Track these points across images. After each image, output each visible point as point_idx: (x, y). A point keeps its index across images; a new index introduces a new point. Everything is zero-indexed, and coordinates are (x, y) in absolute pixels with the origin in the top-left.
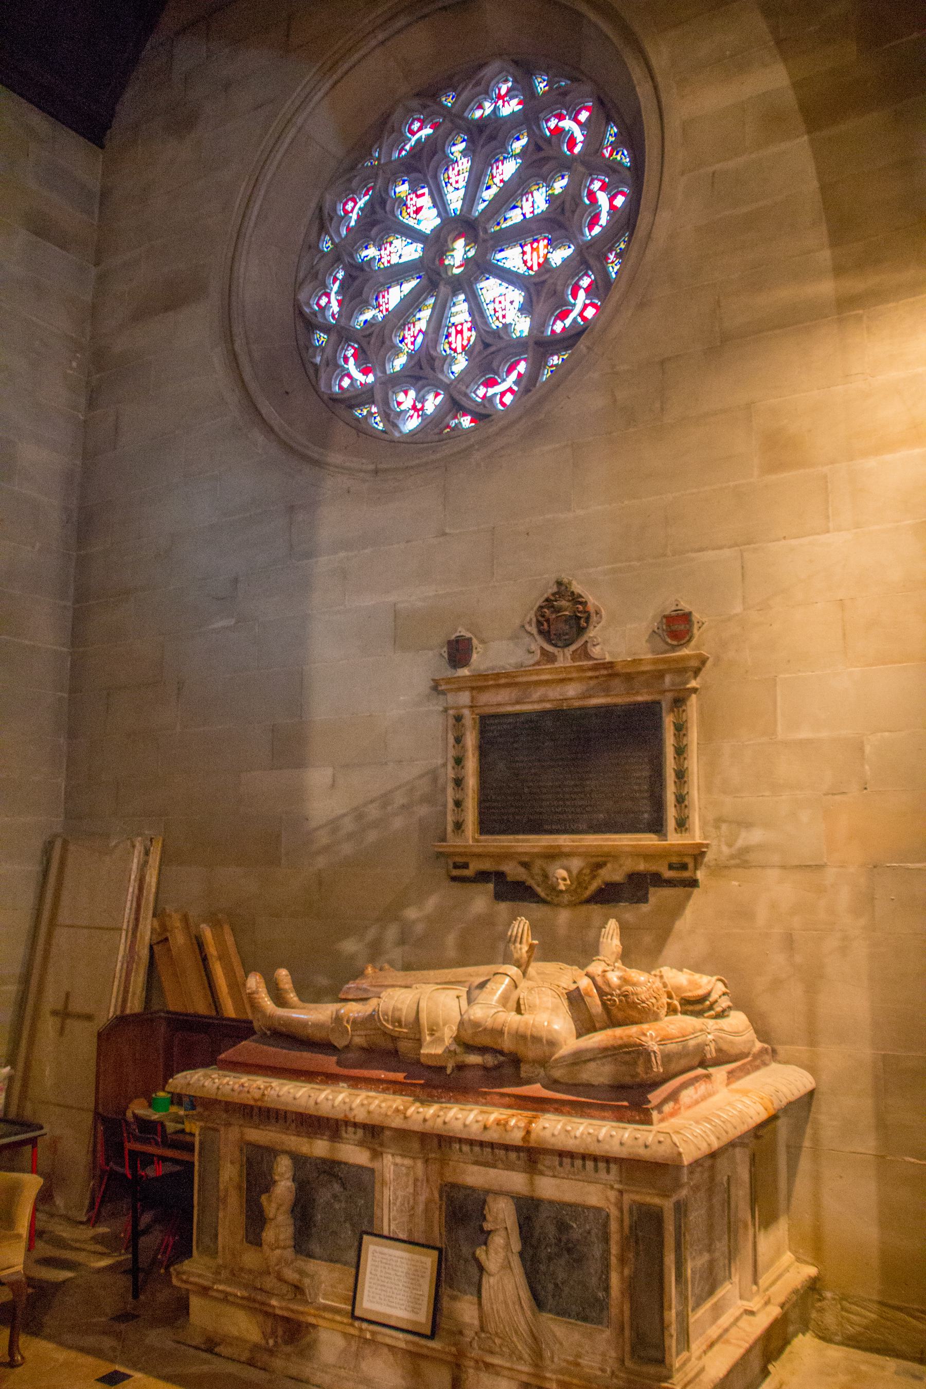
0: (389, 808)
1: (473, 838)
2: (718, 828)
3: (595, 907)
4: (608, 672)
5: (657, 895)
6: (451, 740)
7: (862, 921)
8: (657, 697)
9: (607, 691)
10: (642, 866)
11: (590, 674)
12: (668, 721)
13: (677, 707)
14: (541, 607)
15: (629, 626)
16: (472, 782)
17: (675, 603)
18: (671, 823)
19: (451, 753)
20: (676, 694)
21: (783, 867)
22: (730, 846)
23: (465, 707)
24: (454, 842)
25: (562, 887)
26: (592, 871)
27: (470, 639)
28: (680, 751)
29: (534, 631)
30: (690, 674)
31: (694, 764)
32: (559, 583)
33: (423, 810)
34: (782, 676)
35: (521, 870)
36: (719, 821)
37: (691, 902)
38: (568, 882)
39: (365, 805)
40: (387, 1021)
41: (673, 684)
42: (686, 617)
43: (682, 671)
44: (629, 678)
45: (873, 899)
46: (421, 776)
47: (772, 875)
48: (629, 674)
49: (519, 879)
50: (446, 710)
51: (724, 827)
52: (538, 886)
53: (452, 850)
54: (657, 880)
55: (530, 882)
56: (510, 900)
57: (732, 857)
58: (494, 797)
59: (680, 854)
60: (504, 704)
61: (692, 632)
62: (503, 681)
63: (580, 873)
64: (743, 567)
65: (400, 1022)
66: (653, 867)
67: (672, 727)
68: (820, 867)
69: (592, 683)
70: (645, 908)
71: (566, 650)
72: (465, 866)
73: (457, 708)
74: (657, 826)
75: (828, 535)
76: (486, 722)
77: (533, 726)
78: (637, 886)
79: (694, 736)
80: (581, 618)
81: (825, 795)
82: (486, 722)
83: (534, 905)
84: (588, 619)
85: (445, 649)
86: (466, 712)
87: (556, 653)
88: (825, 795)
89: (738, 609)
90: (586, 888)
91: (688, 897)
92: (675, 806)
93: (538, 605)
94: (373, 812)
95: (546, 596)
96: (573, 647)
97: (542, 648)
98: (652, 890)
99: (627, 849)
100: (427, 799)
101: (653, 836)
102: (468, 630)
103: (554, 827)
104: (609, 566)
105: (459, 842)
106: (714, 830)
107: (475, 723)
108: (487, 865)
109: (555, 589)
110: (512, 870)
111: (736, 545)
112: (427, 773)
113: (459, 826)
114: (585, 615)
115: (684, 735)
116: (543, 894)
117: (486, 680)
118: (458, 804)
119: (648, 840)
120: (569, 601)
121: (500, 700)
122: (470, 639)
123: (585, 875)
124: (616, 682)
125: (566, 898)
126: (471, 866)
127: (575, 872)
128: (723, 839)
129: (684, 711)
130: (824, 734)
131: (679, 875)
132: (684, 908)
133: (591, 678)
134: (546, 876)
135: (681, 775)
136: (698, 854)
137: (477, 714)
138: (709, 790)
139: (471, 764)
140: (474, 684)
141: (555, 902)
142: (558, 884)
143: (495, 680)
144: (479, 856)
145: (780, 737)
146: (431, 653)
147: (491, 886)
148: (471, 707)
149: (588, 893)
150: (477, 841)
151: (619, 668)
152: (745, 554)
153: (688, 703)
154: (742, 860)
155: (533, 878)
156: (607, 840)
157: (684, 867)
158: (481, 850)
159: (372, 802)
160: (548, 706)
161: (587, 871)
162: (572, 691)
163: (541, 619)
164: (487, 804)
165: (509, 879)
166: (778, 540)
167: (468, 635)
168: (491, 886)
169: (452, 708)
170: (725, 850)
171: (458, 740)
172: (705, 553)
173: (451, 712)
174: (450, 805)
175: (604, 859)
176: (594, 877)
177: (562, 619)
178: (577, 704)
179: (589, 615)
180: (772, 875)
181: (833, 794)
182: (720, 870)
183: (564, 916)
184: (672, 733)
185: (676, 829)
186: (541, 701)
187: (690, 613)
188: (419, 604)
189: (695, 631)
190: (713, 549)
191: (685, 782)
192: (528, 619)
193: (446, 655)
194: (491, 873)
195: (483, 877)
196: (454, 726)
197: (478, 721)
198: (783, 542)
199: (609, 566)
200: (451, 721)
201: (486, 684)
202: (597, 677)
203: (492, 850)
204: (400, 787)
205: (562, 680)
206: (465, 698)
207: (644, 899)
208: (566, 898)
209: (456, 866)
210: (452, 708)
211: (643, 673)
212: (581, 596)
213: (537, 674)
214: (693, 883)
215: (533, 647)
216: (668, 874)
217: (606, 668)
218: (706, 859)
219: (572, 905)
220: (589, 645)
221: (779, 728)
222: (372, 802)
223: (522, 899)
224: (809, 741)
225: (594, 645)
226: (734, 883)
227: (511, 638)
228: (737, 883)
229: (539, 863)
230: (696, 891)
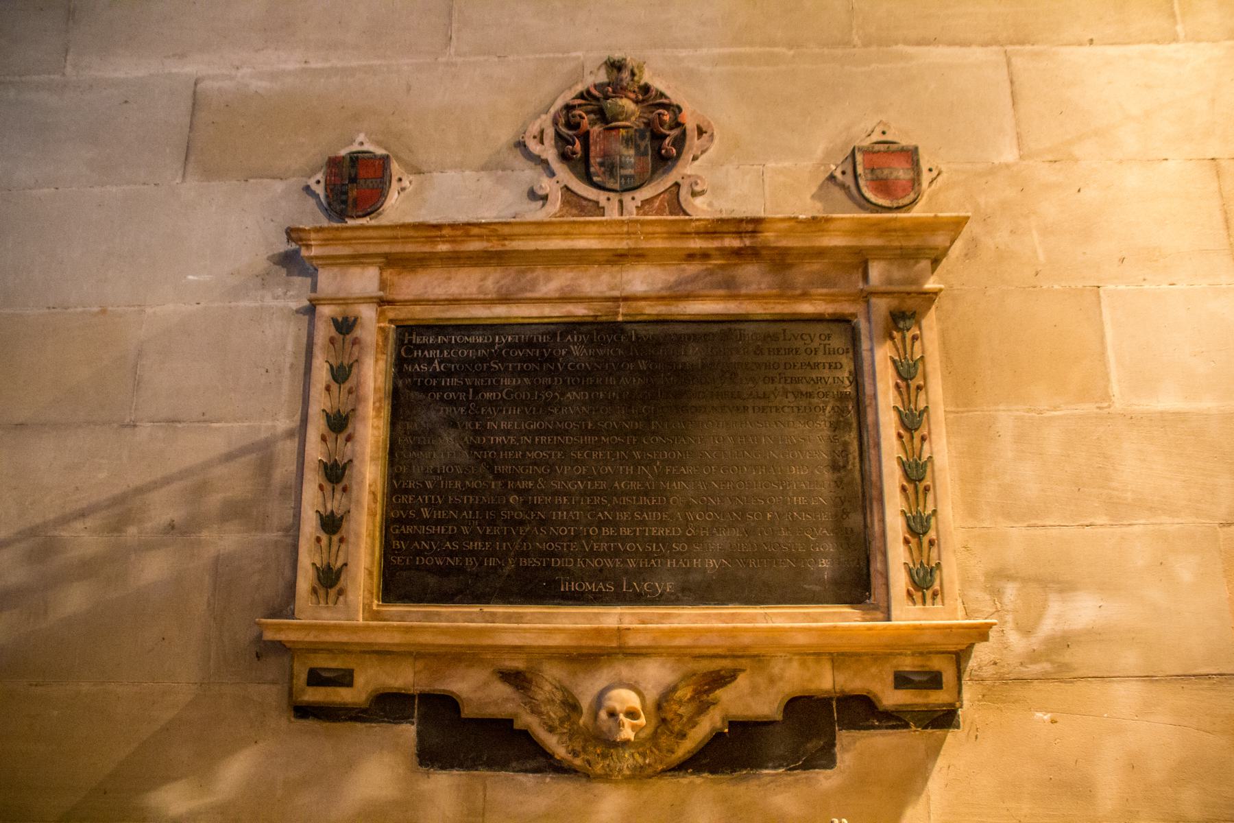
0: (132, 530)
1: (367, 607)
2: (996, 593)
3: (697, 780)
4: (744, 241)
5: (856, 749)
6: (321, 374)
8: (847, 308)
9: (731, 289)
10: (826, 681)
11: (697, 244)
12: (882, 357)
13: (898, 329)
14: (568, 108)
15: (771, 165)
16: (370, 473)
17: (878, 130)
18: (899, 581)
19: (320, 403)
20: (894, 303)
21: (1149, 678)
22: (1027, 632)
23: (367, 300)
24: (312, 617)
25: (627, 733)
26: (698, 693)
27: (385, 160)
28: (912, 422)
29: (549, 152)
30: (925, 264)
31: (942, 450)
32: (615, 66)
33: (227, 540)
34: (1111, 287)
35: (501, 690)
36: (997, 577)
37: (941, 762)
38: (642, 721)
39: (64, 520)
41: (890, 281)
42: (911, 155)
43: (907, 256)
44: (781, 260)
46: (229, 457)
48: (784, 252)
49: (491, 712)
50: (311, 310)
51: (1011, 591)
52: (551, 730)
53: (311, 637)
54: (862, 711)
55: (527, 720)
56: (461, 766)
57: (1033, 657)
58: (426, 513)
59: (925, 652)
60: (472, 301)
61: (920, 184)
62: (475, 246)
63: (667, 695)
64: (1012, 82)
66: (855, 683)
67: (891, 370)
69: (693, 268)
70: (825, 780)
71: (627, 197)
72: (344, 679)
73: (345, 302)
74: (858, 584)
75: (1173, 46)
76: (412, 342)
77: (538, 355)
78: (810, 728)
79: (937, 394)
80: (666, 136)
81: (1222, 525)
82: (412, 342)
83: (529, 780)
84: (680, 142)
85: (320, 176)
86: (368, 313)
87: (603, 202)
88: (1222, 525)
89: (1009, 155)
90: (682, 735)
91: (934, 751)
92: (906, 542)
93: (560, 103)
94: (85, 540)
95: (580, 88)
96: (646, 193)
97: (567, 188)
99: (802, 640)
100: (234, 512)
101: (846, 609)
102: (379, 143)
103: (587, 586)
104: (726, 50)
105: (327, 617)
106: (988, 597)
107: (386, 338)
108: (403, 678)
109: (602, 77)
110: (475, 690)
111: (994, 42)
112: (243, 451)
113: (330, 579)
114: (674, 133)
115: (919, 388)
116: (561, 752)
117: (432, 240)
118: (331, 524)
119: (843, 620)
120: (637, 102)
121: (459, 294)
122: (385, 160)
123: (680, 703)
124: (750, 272)
125: (628, 760)
126: (360, 680)
127: (652, 695)
128: (1009, 618)
129: (915, 338)
130: (1208, 404)
131: (920, 700)
132: (926, 780)
133: (691, 256)
134: (573, 707)
135: (916, 474)
136: (959, 648)
137: (391, 321)
138: (972, 510)
139: (372, 430)
140: (397, 248)
141: (598, 768)
142: (620, 725)
143: (453, 240)
144: (383, 654)
145: (1118, 405)
146: (279, 187)
147: (409, 731)
148: (382, 302)
150: (376, 616)
151: (769, 236)
152: (1017, 62)
153: (924, 323)
154: (1060, 664)
155: (535, 711)
156: (733, 617)
157: (935, 681)
158: (397, 638)
159: (82, 514)
160: (579, 311)
161: (685, 693)
162: (639, 280)
163: (564, 130)
164: (409, 530)
165: (467, 712)
166: (1081, 44)
167: (380, 151)
168: (409, 731)
169: (332, 301)
170: (1015, 640)
171: (341, 374)
172: (932, 48)
173: (326, 311)
174: (310, 525)
175: (728, 663)
176: (703, 708)
177: (617, 132)
178: (652, 310)
179: (684, 133)
180: (1126, 695)
182: (1006, 685)
184: (891, 384)
185: (909, 594)
186: (564, 299)
187: (916, 149)
188: (262, 85)
189: (925, 184)
190: (952, 43)
191: (927, 489)
192: (534, 129)
193: (320, 190)
194: (412, 697)
195: (389, 706)
196: (332, 341)
197: (392, 336)
198: (1087, 49)
199: (726, 50)
200: (324, 332)
201: (427, 248)
202: (705, 255)
203: (427, 639)
204: (167, 481)
205: (619, 258)
206: (365, 280)
207: (825, 758)
208: (628, 760)
209: (316, 678)
210: (332, 301)
211: (820, 253)
212: (662, 95)
213: (567, 235)
214: (945, 718)
215: (546, 185)
216: (891, 698)
217: (739, 234)
218: (972, 663)
219: (640, 775)
220: (684, 193)
221: (1115, 389)
222: (82, 514)
223: (495, 763)
224: (1181, 417)
225: (694, 194)
226: (1039, 715)
227: (484, 168)
228: (1047, 717)
229: (553, 673)
230: (951, 736)
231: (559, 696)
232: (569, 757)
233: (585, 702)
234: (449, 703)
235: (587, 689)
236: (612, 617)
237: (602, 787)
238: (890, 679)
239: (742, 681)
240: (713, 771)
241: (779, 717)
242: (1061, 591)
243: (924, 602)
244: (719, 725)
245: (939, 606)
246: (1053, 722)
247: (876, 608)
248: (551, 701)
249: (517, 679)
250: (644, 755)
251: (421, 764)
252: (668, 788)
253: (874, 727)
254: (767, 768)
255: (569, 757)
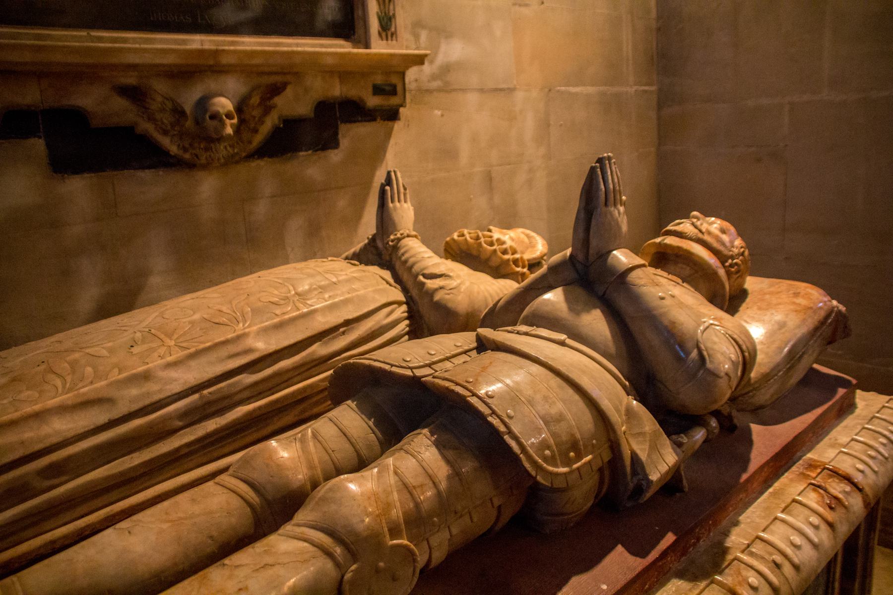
5: (351, 135)
7: (542, 150)
10: (337, 91)
21: (482, 91)
26: (263, 100)
35: (120, 103)
37: (392, 141)
40: (552, 460)
45: (549, 125)
47: (472, 98)
52: (165, 133)
55: (146, 127)
57: (434, 77)
65: (574, 445)
66: (352, 92)
68: (511, 90)
70: (335, 156)
83: (146, 175)
90: (256, 131)
91: (388, 135)
98: (343, 128)
101: (341, 42)
116: (174, 149)
132: (385, 152)
134: (179, 112)
142: (223, 125)
147: (38, 145)
149: (258, 139)
155: (151, 119)
161: (255, 100)
168: (38, 145)
176: (267, 110)
181: (520, 5)
183: (207, 187)
207: (331, 143)
208: (222, 151)
216: (373, 101)
230: (397, 126)
231: (169, 105)
232: (181, 153)
233: (188, 109)
234: (78, 116)
235: (189, 98)
236: (198, 41)
237: (200, 174)
238: (370, 90)
239: (289, 91)
240: (271, 156)
241: (312, 115)
242: (446, 37)
243: (387, 40)
244: (277, 122)
245: (394, 42)
246: (442, 115)
247: (359, 42)
248: (163, 110)
249: (136, 94)
250: (232, 146)
251: (55, 172)
252: (244, 171)
253: (359, 121)
254: (301, 151)
255: (181, 153)
